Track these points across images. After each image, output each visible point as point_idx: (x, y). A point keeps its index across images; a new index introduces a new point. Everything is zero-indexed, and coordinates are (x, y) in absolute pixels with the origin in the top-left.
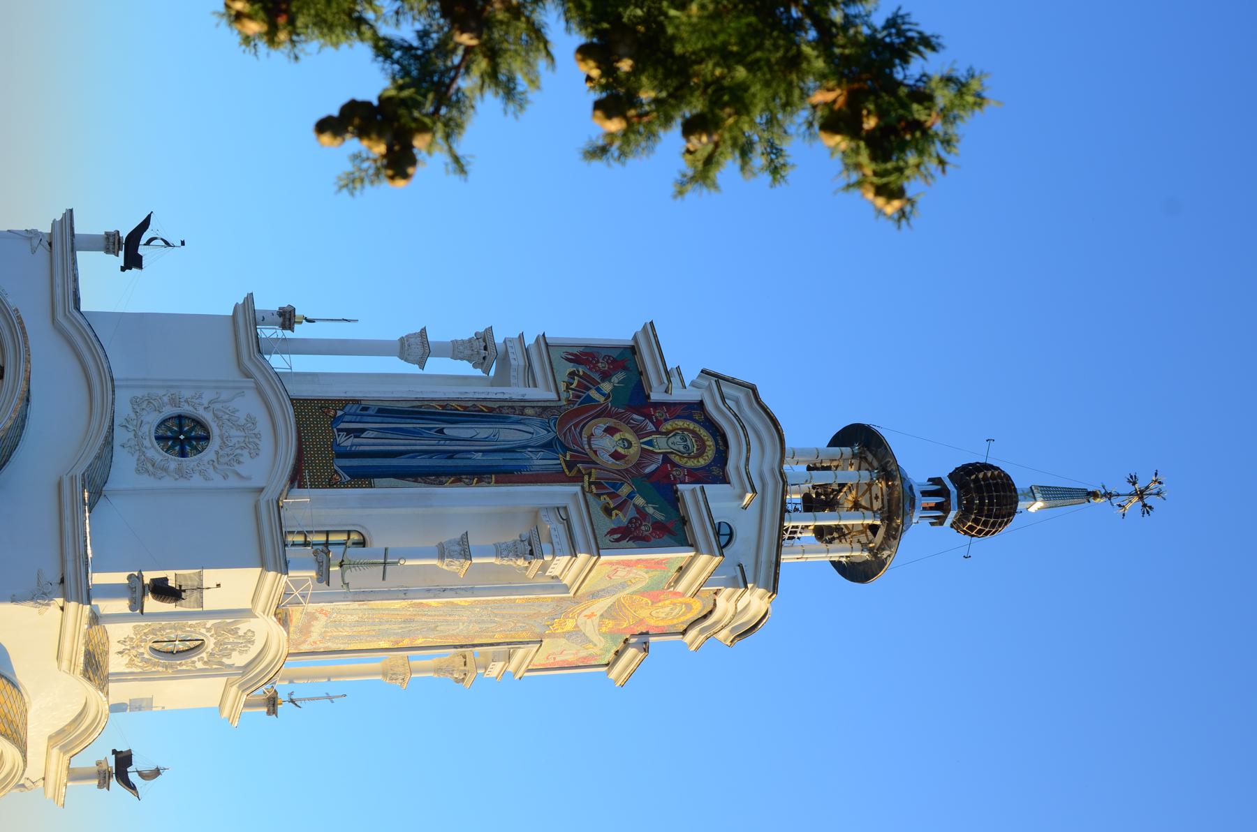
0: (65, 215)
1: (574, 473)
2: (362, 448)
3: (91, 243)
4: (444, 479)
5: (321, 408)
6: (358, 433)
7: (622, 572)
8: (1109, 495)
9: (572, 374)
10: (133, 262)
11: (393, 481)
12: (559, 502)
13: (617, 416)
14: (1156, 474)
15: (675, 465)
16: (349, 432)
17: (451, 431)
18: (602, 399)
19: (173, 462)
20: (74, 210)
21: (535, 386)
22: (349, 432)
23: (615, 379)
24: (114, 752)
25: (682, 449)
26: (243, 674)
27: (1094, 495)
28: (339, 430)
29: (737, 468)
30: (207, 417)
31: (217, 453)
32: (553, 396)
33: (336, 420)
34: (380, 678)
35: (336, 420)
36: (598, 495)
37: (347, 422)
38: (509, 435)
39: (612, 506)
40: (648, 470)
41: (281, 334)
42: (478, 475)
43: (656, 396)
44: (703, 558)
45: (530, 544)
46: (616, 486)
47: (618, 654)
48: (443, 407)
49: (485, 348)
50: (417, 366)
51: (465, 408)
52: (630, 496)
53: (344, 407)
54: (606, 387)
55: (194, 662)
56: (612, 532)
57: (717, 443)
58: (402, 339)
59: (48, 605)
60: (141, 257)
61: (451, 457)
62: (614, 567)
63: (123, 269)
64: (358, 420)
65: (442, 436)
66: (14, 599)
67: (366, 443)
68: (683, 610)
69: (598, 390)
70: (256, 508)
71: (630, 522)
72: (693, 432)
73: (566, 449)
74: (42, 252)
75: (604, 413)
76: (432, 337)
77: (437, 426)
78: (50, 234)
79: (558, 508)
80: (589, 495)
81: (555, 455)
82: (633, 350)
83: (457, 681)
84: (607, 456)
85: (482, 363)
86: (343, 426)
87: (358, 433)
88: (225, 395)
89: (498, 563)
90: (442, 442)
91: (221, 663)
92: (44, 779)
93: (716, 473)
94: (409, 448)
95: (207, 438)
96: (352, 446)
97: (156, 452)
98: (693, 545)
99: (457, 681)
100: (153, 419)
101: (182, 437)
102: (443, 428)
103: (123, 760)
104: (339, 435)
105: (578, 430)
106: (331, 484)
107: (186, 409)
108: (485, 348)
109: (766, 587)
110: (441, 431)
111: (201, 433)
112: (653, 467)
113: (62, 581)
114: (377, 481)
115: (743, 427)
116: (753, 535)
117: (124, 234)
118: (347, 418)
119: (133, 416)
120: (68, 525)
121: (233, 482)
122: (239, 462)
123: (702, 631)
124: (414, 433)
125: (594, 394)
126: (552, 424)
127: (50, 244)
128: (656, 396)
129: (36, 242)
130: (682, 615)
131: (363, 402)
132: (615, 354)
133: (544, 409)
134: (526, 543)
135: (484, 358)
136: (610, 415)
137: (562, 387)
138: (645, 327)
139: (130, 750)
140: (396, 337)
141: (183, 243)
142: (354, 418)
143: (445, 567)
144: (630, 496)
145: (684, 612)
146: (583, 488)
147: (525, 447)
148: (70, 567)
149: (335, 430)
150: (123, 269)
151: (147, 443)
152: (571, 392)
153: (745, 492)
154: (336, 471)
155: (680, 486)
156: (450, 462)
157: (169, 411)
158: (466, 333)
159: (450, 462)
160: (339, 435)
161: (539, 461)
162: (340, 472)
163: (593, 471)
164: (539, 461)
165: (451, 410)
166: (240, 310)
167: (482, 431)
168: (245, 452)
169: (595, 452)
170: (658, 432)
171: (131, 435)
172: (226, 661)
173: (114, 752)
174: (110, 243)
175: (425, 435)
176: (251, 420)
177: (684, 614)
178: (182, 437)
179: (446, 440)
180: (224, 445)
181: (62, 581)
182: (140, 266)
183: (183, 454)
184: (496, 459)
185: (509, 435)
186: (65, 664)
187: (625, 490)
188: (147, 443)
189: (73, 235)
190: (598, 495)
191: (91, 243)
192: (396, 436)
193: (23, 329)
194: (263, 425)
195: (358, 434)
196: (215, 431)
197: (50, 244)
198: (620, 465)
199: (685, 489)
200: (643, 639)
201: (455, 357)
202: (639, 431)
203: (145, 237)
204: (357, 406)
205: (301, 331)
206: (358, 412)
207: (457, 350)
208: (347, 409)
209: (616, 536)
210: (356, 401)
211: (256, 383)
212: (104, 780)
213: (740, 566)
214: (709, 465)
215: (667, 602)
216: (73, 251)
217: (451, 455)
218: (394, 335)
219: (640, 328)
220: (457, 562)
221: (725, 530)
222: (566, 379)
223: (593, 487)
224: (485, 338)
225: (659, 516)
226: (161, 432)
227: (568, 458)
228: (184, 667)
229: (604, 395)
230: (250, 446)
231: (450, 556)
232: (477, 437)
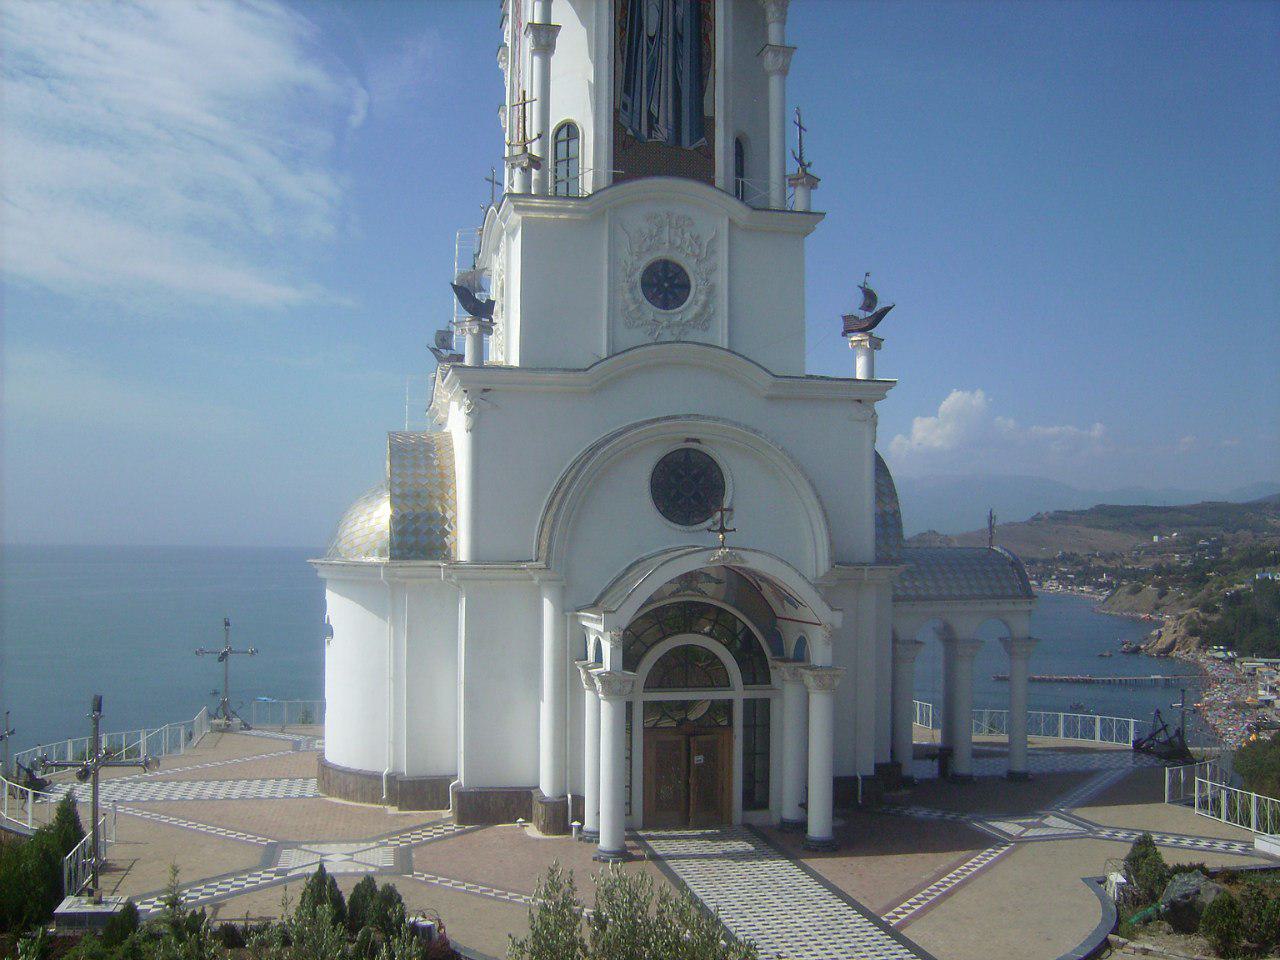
2: (671, 119)
11: (706, 102)
16: (651, 128)
35: (638, 133)
37: (640, 128)
48: (623, 29)
61: (681, 38)
77: (645, 43)
86: (644, 132)
87: (652, 120)
94: (670, 74)
97: (690, 309)
100: (651, 311)
107: (638, 276)
110: (651, 39)
113: (860, 401)
124: (653, 62)
142: (636, 115)
157: (639, 293)
162: (698, 144)
179: (661, 37)
181: (860, 401)
197: (485, 390)
210: (616, 113)
217: (678, 37)
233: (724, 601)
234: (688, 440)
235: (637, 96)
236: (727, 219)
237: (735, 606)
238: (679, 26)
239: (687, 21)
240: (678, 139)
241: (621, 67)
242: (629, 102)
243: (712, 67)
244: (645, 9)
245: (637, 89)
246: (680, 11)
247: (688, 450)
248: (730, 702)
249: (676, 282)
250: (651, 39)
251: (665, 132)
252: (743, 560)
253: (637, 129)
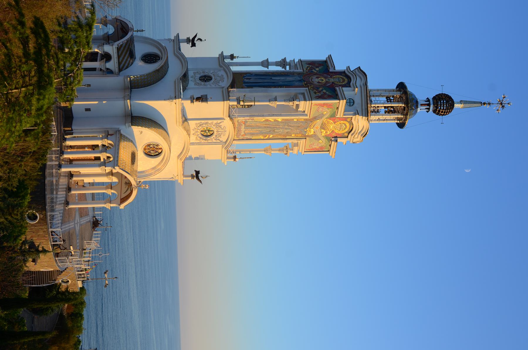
0: (177, 35)
1: (306, 86)
3: (183, 41)
4: (271, 87)
6: (249, 79)
7: (321, 109)
8: (489, 104)
9: (308, 67)
10: (194, 45)
12: (302, 92)
13: (320, 75)
14: (504, 95)
15: (335, 84)
17: (273, 78)
18: (316, 72)
19: (203, 83)
20: (179, 34)
21: (298, 69)
22: (247, 79)
23: (320, 68)
24: (195, 171)
25: (338, 81)
26: (225, 144)
27: (484, 104)
29: (353, 84)
30: (212, 75)
31: (213, 81)
32: (302, 71)
33: (244, 77)
34: (263, 152)
35: (244, 77)
36: (313, 90)
38: (289, 79)
39: (317, 92)
40: (327, 85)
41: (231, 61)
42: (281, 86)
43: (331, 70)
44: (341, 101)
45: (293, 99)
46: (318, 88)
47: (330, 146)
48: (272, 74)
49: (284, 62)
50: (267, 68)
51: (278, 74)
52: (322, 90)
54: (317, 69)
55: (212, 139)
56: (316, 97)
57: (348, 80)
58: (262, 62)
59: (172, 101)
60: (195, 44)
62: (318, 106)
63: (191, 47)
66: (165, 100)
67: (251, 81)
68: (344, 126)
69: (315, 70)
70: (223, 91)
71: (321, 95)
72: (341, 78)
73: (304, 81)
74: (172, 43)
75: (316, 74)
76: (269, 61)
78: (174, 39)
79: (302, 93)
80: (310, 90)
81: (302, 83)
82: (326, 62)
83: (285, 154)
84: (316, 83)
85: (284, 66)
86: (246, 78)
87: (249, 79)
88: (216, 71)
89: (285, 104)
91: (219, 140)
92: (178, 175)
93: (348, 85)
95: (211, 79)
96: (248, 81)
97: (199, 82)
98: (339, 100)
99: (285, 154)
100: (198, 76)
103: (197, 173)
105: (309, 78)
106: (242, 88)
107: (206, 74)
108: (284, 62)
109: (365, 116)
110: (271, 78)
111: (210, 78)
112: (329, 85)
114: (254, 87)
115: (356, 76)
116: (360, 102)
117: (191, 38)
118: (247, 76)
120: (177, 87)
121: (217, 86)
122: (219, 83)
123: (352, 135)
125: (313, 70)
126: (301, 76)
127: (174, 41)
128: (330, 70)
129: (170, 41)
130: (344, 129)
132: (320, 63)
133: (299, 74)
135: (284, 65)
136: (318, 75)
137: (305, 69)
138: (329, 56)
139: (199, 171)
140: (261, 61)
141: (205, 40)
143: (271, 105)
144: (322, 90)
145: (345, 128)
146: (309, 89)
147: (293, 81)
148: (177, 94)
150: (191, 47)
152: (307, 70)
153: (355, 88)
155: (336, 88)
156: (273, 84)
158: (279, 59)
159: (273, 84)
161: (297, 84)
163: (312, 85)
164: (297, 84)
166: (220, 56)
167: (282, 78)
168: (221, 81)
169: (313, 82)
170: (331, 78)
171: (193, 79)
172: (220, 139)
173: (195, 171)
174: (188, 40)
177: (345, 129)
180: (215, 80)
182: (195, 46)
183: (205, 82)
184: (286, 83)
185: (289, 79)
186: (178, 123)
187: (320, 89)
189: (179, 39)
190: (313, 90)
191: (183, 41)
193: (166, 50)
194: (225, 76)
196: (213, 77)
197: (174, 41)
198: (320, 84)
199: (337, 88)
200: (336, 139)
201: (277, 66)
202: (325, 78)
203: (196, 39)
205: (235, 60)
207: (277, 64)
208: (247, 74)
209: (317, 98)
211: (224, 68)
212: (192, 177)
213: (357, 110)
214: (346, 84)
215: (338, 123)
216: (179, 43)
217: (274, 83)
218: (260, 60)
219: (328, 56)
220: (274, 103)
221: (352, 101)
222: (306, 68)
223: (312, 89)
224: (284, 60)
225: (330, 94)
226: (200, 79)
227: (305, 83)
228: (209, 141)
229: (316, 71)
231: (272, 101)
234: (162, 58)
239: (279, 84)
240: (244, 83)
246: (281, 83)
250: (271, 78)
251: (247, 81)
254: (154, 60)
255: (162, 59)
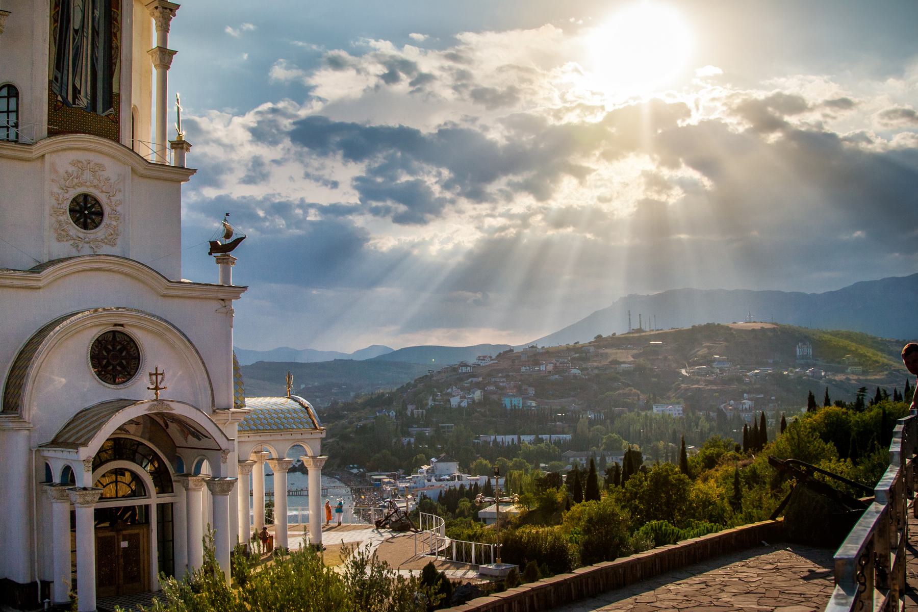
4: (114, 45)
5: (55, 110)
16: (75, 97)
17: (76, 23)
22: (75, 97)
28: (74, 103)
31: (102, 191)
35: (65, 101)
45: (166, 8)
48: (56, 21)
53: (55, 94)
64: (66, 87)
65: (80, 32)
67: (85, 89)
87: (76, 92)
90: (85, 34)
96: (87, 99)
100: (75, 230)
101: (86, 212)
102: (74, 28)
104: (78, 105)
107: (66, 205)
110: (76, 31)
113: (223, 300)
114: (115, 90)
118: (64, 94)
119: (72, 242)
131: (51, 78)
134: (165, 10)
149: (74, 106)
151: (92, 236)
154: (107, 116)
156: (102, 35)
159: (102, 35)
160: (78, 105)
162: (107, 113)
165: (58, 16)
175: (79, 44)
176: (75, 163)
178: (86, 212)
181: (223, 300)
188: (92, 236)
192: (80, 65)
195: (77, 92)
204: (54, 85)
206: (58, 85)
210: (50, 82)
217: (95, 32)
230: (97, 168)
232: (81, 6)
233: (141, 437)
234: (116, 325)
235: (65, 72)
236: (130, 167)
237: (150, 440)
238: (97, 28)
241: (54, 49)
242: (59, 76)
243: (119, 58)
244: (72, 9)
245: (66, 67)
246: (97, 13)
247: (114, 332)
248: (147, 507)
249: (93, 210)
250: (76, 31)
251: (85, 100)
252: (172, 409)
253: (65, 97)
254: (114, 348)
255: (122, 325)
